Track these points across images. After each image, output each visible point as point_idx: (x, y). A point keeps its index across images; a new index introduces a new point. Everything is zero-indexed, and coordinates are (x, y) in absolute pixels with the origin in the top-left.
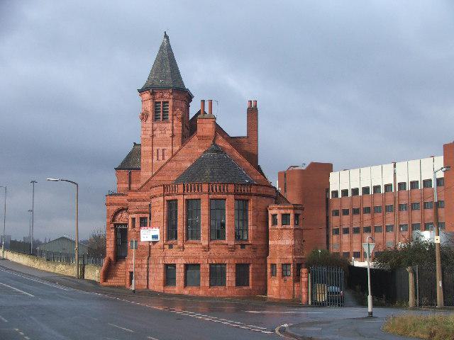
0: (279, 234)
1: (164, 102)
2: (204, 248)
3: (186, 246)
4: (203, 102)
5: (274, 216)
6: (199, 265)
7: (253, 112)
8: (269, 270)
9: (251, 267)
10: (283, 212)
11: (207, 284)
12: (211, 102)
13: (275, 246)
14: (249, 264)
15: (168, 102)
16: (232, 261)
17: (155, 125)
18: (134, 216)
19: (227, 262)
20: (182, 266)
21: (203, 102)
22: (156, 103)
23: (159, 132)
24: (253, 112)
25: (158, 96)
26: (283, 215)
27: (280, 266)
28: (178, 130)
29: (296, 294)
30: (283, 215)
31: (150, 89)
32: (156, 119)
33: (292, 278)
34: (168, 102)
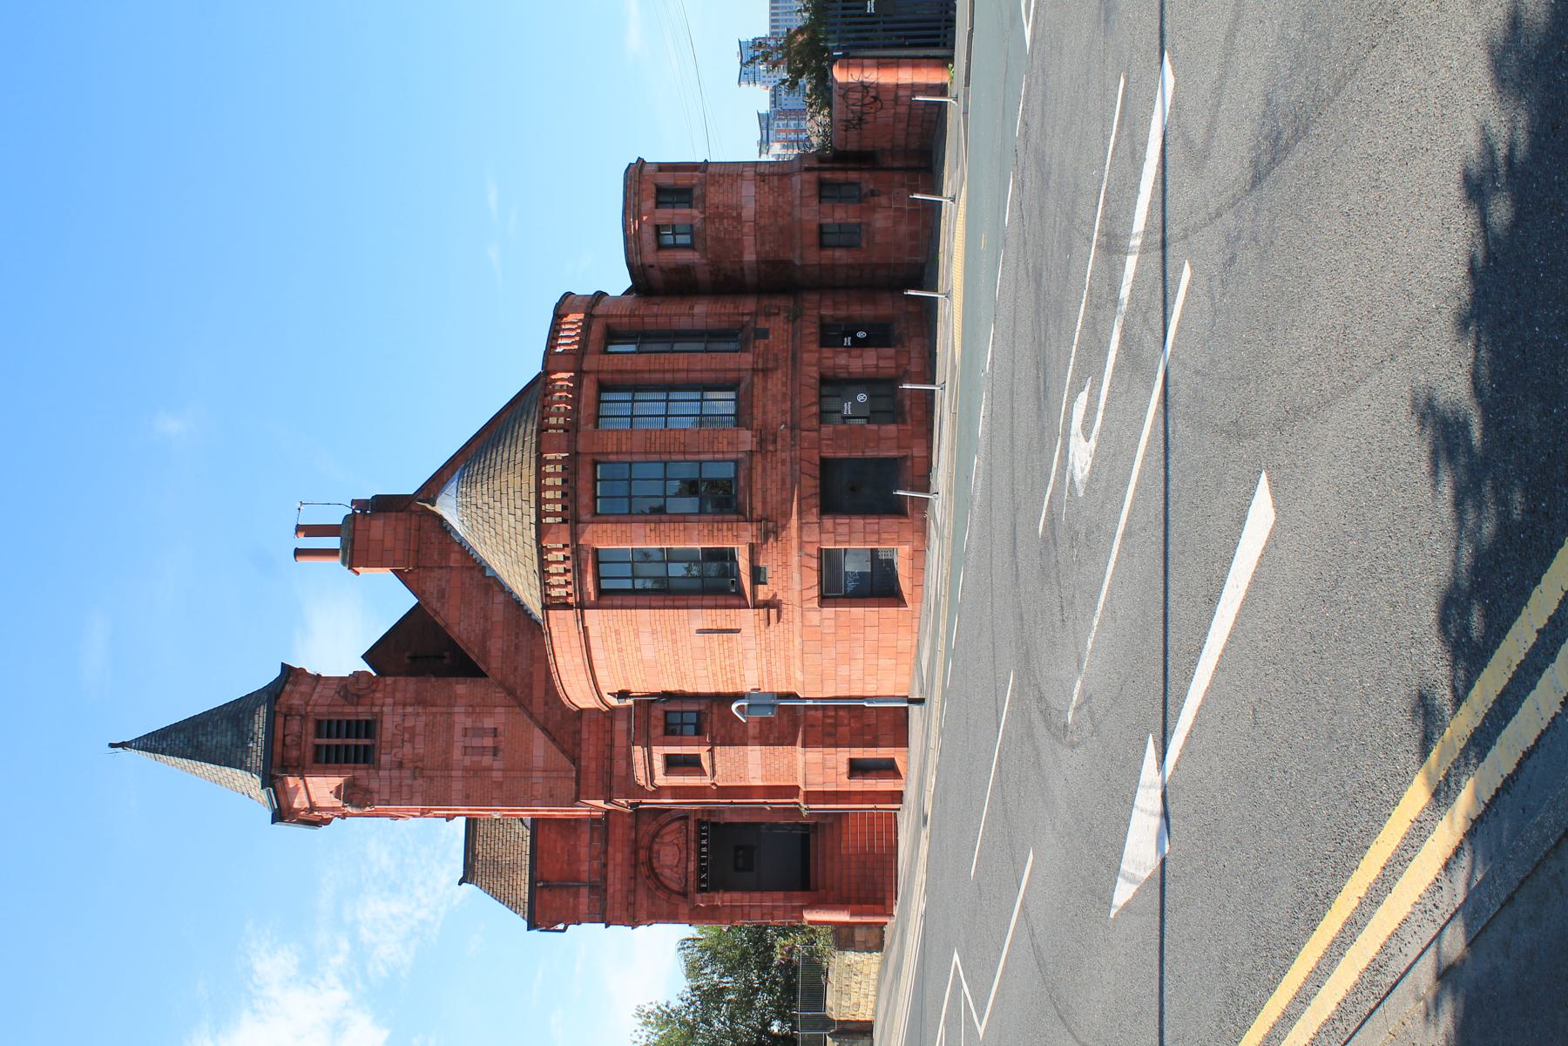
0: (721, 217)
1: (318, 735)
2: (762, 442)
4: (299, 553)
10: (649, 204)
12: (300, 529)
13: (759, 229)
14: (821, 318)
15: (319, 723)
17: (385, 759)
18: (659, 764)
19: (814, 372)
20: (828, 522)
21: (299, 553)
22: (316, 760)
23: (407, 748)
28: (408, 686)
29: (914, 163)
30: (658, 204)
32: (365, 756)
33: (866, 175)
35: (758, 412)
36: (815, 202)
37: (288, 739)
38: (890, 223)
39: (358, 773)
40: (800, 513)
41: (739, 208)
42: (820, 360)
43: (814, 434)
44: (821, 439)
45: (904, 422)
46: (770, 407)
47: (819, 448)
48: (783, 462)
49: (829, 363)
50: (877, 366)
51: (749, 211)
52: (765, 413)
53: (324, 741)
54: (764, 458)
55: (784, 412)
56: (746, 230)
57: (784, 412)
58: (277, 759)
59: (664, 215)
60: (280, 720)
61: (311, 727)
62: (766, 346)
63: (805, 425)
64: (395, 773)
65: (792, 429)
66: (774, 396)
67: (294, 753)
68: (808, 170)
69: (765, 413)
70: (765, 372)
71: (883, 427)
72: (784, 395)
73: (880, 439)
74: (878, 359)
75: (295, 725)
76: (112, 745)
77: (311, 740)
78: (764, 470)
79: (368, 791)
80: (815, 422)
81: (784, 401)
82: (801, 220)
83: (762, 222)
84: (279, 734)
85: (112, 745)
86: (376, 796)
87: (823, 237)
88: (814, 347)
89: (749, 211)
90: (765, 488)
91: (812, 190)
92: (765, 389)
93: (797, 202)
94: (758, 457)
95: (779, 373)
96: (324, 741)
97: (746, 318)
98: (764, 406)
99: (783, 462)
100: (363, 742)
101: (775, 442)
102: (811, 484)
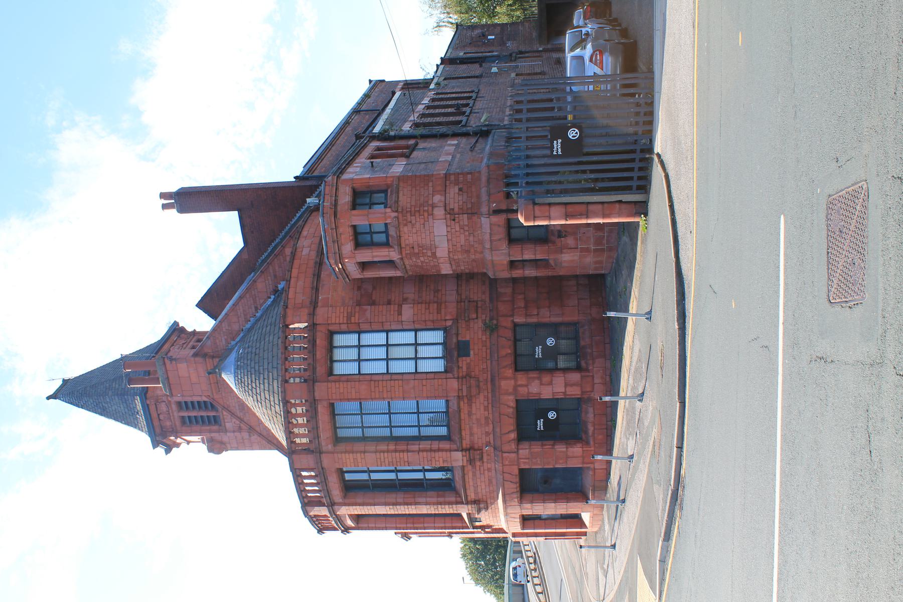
0: (417, 255)
2: (471, 461)
3: (472, 496)
5: (364, 266)
6: (521, 471)
7: (189, 200)
8: (530, 272)
9: (519, 320)
10: (348, 247)
11: (577, 450)
13: (451, 261)
14: (513, 321)
16: (506, 384)
19: (510, 401)
24: (189, 200)
25: (168, 423)
26: (358, 245)
27: (516, 249)
31: (163, 437)
32: (216, 420)
34: (179, 404)
35: (466, 434)
36: (504, 245)
37: (162, 417)
38: (576, 258)
39: (213, 435)
40: (504, 501)
41: (433, 248)
42: (516, 387)
43: (513, 455)
44: (518, 459)
45: (587, 443)
46: (475, 430)
47: (518, 465)
48: (489, 470)
49: (523, 391)
50: (564, 393)
51: (442, 252)
52: (471, 434)
53: (185, 414)
54: (474, 466)
55: (487, 434)
56: (442, 260)
57: (487, 434)
58: (158, 430)
59: (360, 219)
60: (152, 408)
61: (174, 407)
62: (468, 365)
63: (506, 448)
64: (237, 434)
65: (495, 448)
66: (477, 420)
67: (168, 423)
68: (497, 212)
69: (471, 434)
70: (470, 399)
71: (570, 449)
72: (487, 418)
73: (567, 457)
74: (566, 385)
75: (163, 407)
76: (48, 398)
77: (177, 414)
78: (474, 475)
79: (222, 443)
80: (513, 446)
81: (487, 424)
82: (492, 261)
83: (456, 257)
84: (154, 415)
85: (48, 398)
86: (228, 445)
87: (512, 264)
88: (509, 372)
89: (442, 252)
90: (476, 485)
91: (501, 233)
92: (470, 414)
93: (488, 246)
94: (470, 467)
95: (481, 397)
96: (185, 414)
97: (449, 323)
98: (471, 429)
99: (489, 470)
100: (212, 414)
101: (481, 459)
102: (514, 487)
